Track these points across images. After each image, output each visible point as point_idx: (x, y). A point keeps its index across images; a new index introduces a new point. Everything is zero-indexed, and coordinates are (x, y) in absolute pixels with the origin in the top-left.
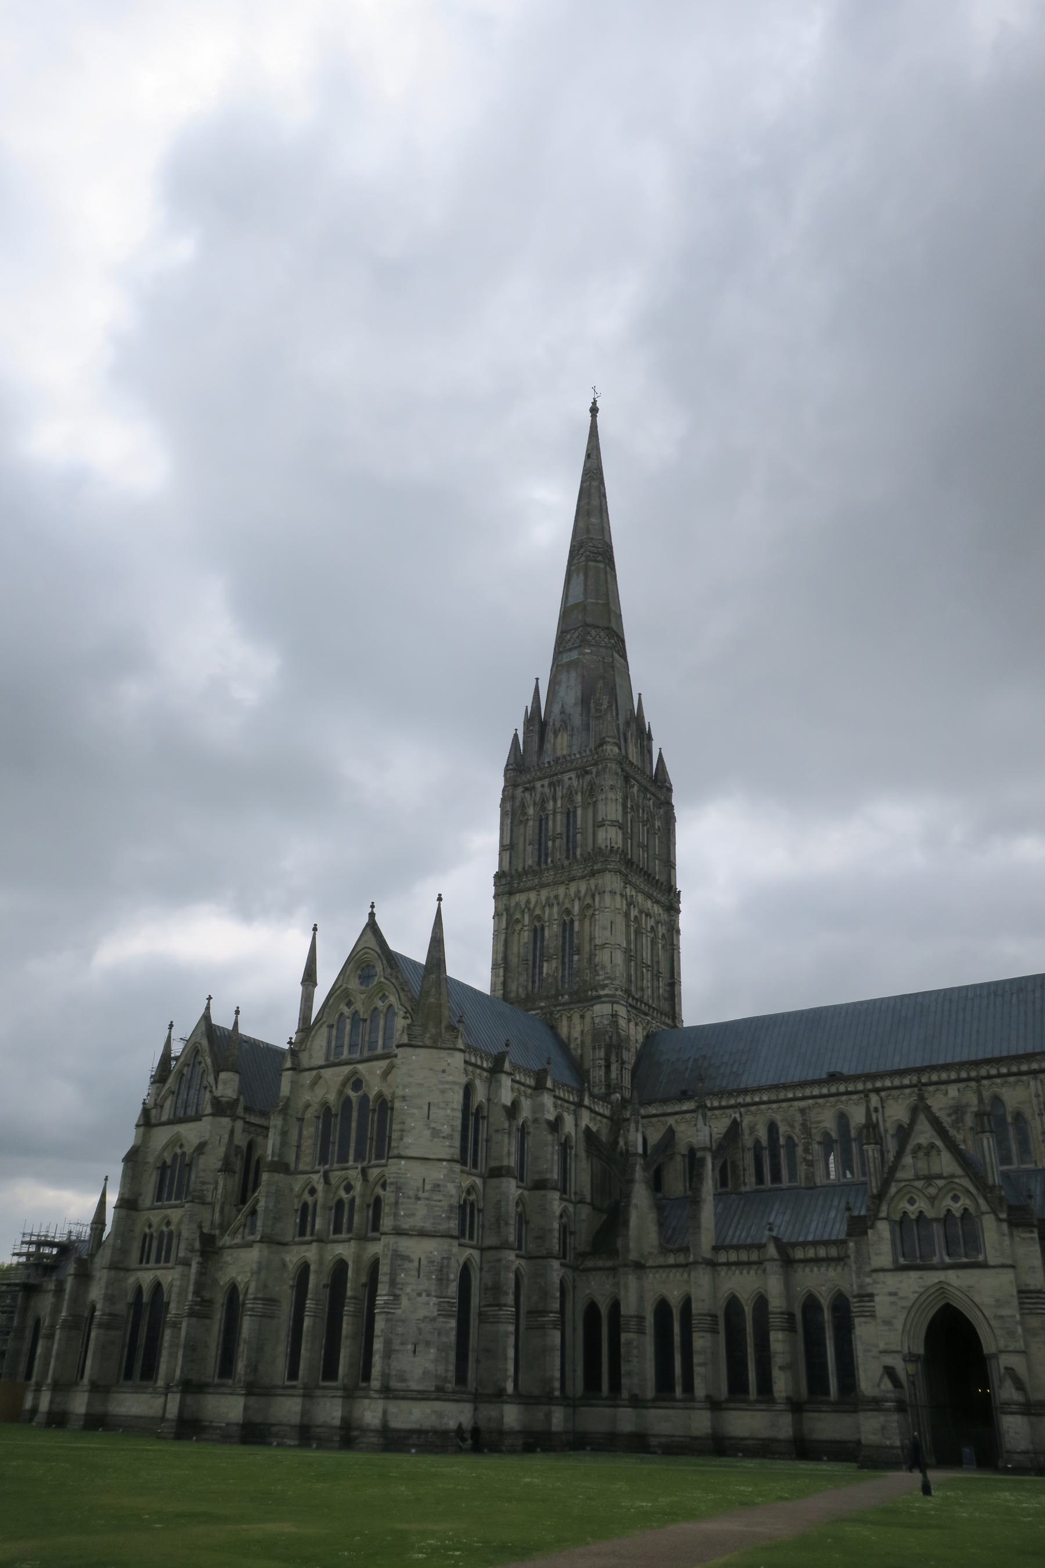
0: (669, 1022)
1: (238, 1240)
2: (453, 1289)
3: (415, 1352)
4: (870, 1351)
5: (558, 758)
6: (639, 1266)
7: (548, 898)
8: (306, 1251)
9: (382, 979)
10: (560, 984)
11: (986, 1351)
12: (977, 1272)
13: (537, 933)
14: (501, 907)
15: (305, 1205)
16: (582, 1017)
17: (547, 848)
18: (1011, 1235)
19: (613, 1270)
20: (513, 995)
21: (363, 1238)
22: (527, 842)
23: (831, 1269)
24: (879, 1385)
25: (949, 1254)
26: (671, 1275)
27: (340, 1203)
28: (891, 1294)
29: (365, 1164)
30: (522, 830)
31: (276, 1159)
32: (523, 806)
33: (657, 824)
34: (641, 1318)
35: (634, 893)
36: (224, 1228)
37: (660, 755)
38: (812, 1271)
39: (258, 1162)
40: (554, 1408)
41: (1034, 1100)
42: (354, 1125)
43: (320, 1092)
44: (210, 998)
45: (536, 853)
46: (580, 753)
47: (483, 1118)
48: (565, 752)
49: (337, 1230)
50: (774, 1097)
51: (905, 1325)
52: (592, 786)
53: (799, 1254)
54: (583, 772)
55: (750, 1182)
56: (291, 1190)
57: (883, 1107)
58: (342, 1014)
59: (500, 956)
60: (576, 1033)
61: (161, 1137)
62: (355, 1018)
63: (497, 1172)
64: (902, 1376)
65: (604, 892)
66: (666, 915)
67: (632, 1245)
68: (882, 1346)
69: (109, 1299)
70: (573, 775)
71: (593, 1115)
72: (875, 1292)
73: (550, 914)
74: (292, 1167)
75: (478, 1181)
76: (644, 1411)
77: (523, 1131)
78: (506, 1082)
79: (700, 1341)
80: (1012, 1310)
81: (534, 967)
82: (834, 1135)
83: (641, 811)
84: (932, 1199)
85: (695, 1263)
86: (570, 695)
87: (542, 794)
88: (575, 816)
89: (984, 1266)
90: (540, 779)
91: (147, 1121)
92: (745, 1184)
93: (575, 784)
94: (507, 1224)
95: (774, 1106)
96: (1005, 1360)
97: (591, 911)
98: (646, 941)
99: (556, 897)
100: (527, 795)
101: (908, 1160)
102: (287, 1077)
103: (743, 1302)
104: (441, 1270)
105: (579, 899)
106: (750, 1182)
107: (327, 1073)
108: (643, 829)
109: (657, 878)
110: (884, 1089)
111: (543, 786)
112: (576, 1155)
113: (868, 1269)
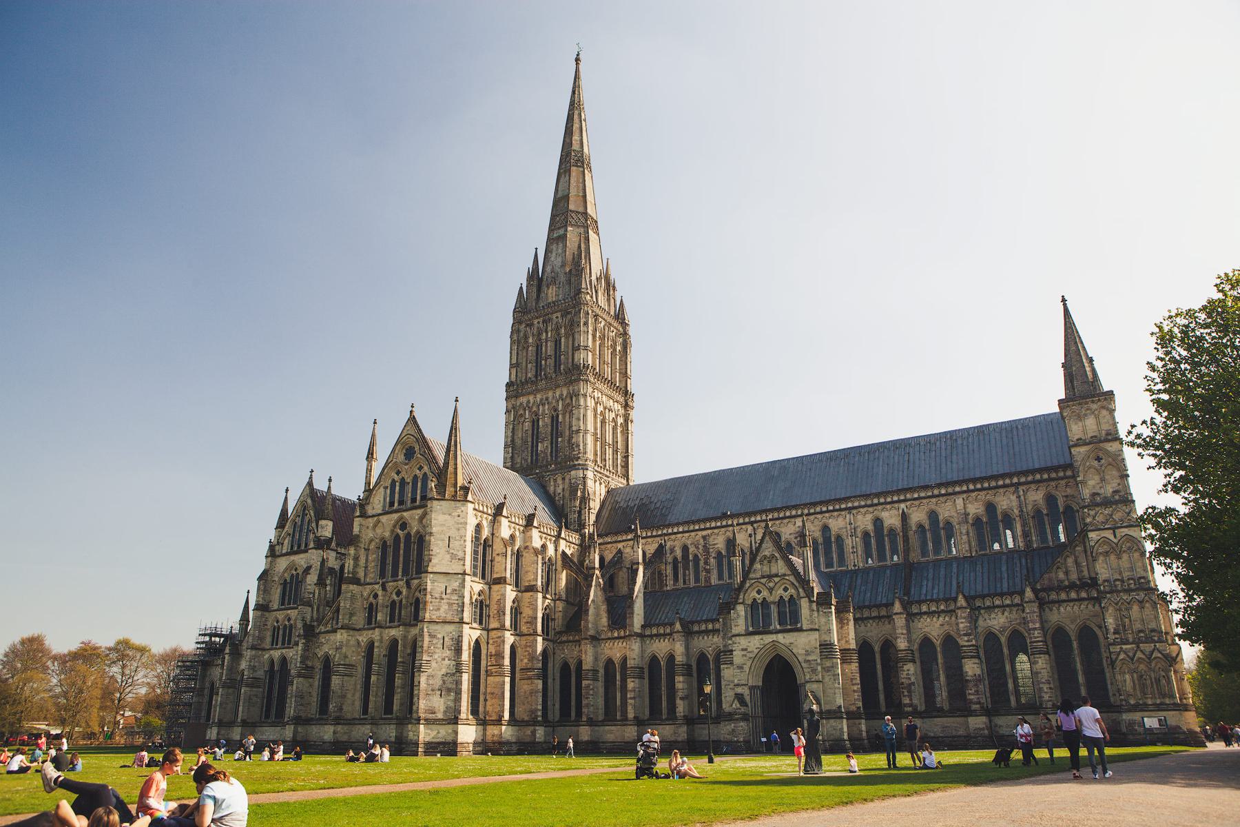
0: (625, 482)
4: (729, 685)
5: (550, 303)
6: (595, 639)
7: (541, 400)
8: (372, 634)
9: (419, 456)
10: (549, 457)
11: (798, 682)
12: (796, 634)
13: (535, 423)
14: (510, 406)
15: (371, 604)
16: (564, 479)
17: (541, 365)
18: (818, 611)
20: (518, 465)
21: (408, 625)
23: (715, 637)
24: (731, 706)
26: (616, 644)
27: (394, 602)
28: (743, 650)
29: (408, 577)
32: (526, 337)
33: (619, 348)
34: (595, 671)
35: (600, 395)
36: (320, 621)
37: (621, 301)
38: (703, 638)
40: (537, 728)
41: (848, 526)
42: (402, 552)
43: (379, 531)
44: (312, 471)
45: (534, 369)
46: (564, 300)
47: (489, 546)
48: (554, 299)
49: (392, 620)
50: (686, 529)
51: (750, 668)
54: (565, 313)
55: (670, 585)
56: (362, 595)
57: (755, 534)
58: (394, 480)
59: (509, 439)
60: (559, 490)
61: (282, 563)
62: (403, 481)
63: (501, 581)
64: (748, 699)
65: (579, 395)
66: (623, 411)
67: (590, 626)
68: (736, 681)
69: (253, 668)
70: (559, 314)
71: (568, 544)
72: (734, 649)
73: (544, 410)
74: (362, 579)
75: (486, 587)
76: (597, 728)
77: (518, 555)
78: (504, 522)
79: (631, 684)
80: (815, 656)
81: (532, 447)
82: (724, 553)
83: (606, 339)
84: (771, 590)
85: (630, 635)
88: (560, 344)
89: (801, 630)
91: (272, 553)
92: (667, 586)
93: (560, 321)
94: (504, 614)
95: (687, 535)
96: (808, 686)
97: (570, 408)
98: (609, 429)
99: (547, 399)
101: (757, 566)
102: (357, 522)
103: (660, 659)
104: (458, 644)
105: (562, 400)
107: (384, 519)
108: (608, 352)
109: (618, 385)
110: (756, 522)
111: (539, 323)
112: (556, 570)
113: (730, 635)
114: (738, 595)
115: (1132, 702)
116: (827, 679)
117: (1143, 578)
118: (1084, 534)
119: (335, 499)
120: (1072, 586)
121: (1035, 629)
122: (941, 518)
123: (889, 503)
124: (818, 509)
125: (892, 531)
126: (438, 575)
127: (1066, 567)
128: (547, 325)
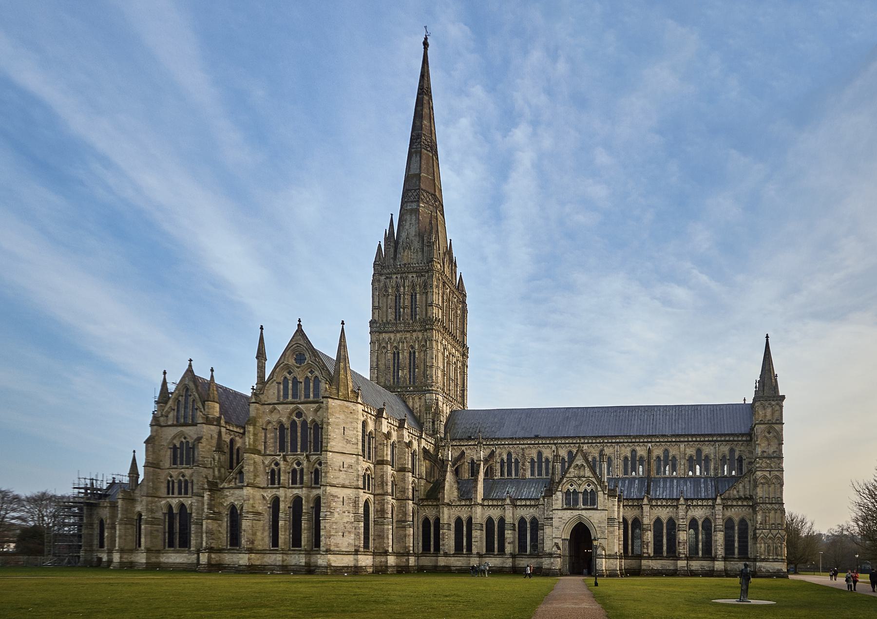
1: (232, 485)
2: (361, 510)
3: (343, 536)
4: (549, 537)
5: (405, 264)
12: (594, 511)
18: (608, 499)
19: (437, 505)
22: (389, 307)
25: (583, 505)
30: (385, 300)
31: (252, 447)
32: (386, 286)
39: (238, 450)
41: (616, 453)
46: (418, 263)
52: (425, 284)
53: (519, 503)
54: (420, 273)
68: (554, 536)
86: (412, 230)
87: (397, 282)
89: (596, 509)
90: (395, 273)
94: (387, 485)
100: (388, 280)
101: (571, 470)
106: (498, 476)
111: (397, 277)
114: (558, 486)
115: (763, 557)
116: (610, 537)
117: (780, 498)
118: (751, 472)
119: (219, 387)
120: (740, 499)
121: (719, 518)
122: (670, 454)
123: (642, 442)
124: (598, 441)
125: (641, 457)
126: (336, 454)
127: (739, 488)
128: (404, 281)
